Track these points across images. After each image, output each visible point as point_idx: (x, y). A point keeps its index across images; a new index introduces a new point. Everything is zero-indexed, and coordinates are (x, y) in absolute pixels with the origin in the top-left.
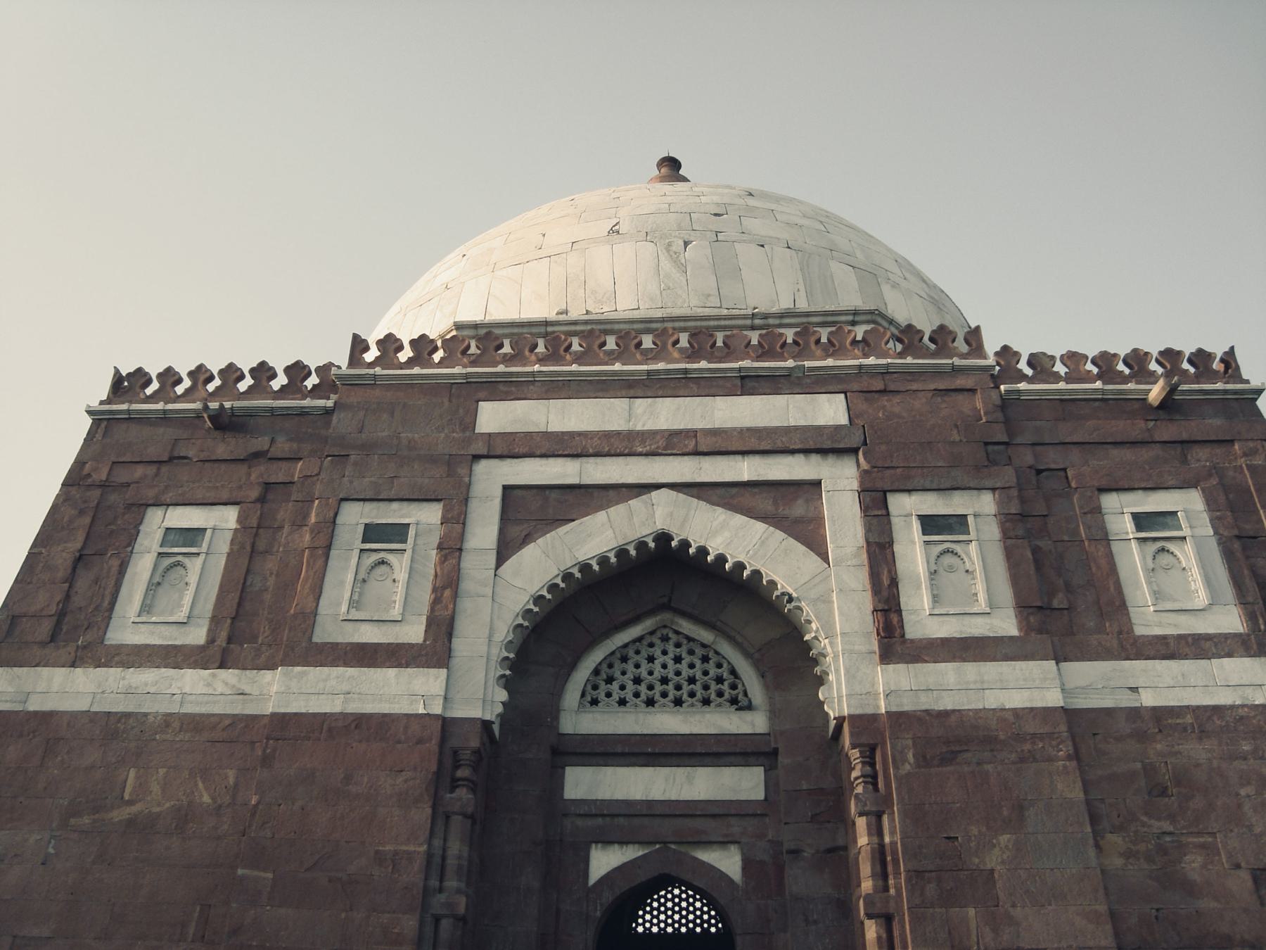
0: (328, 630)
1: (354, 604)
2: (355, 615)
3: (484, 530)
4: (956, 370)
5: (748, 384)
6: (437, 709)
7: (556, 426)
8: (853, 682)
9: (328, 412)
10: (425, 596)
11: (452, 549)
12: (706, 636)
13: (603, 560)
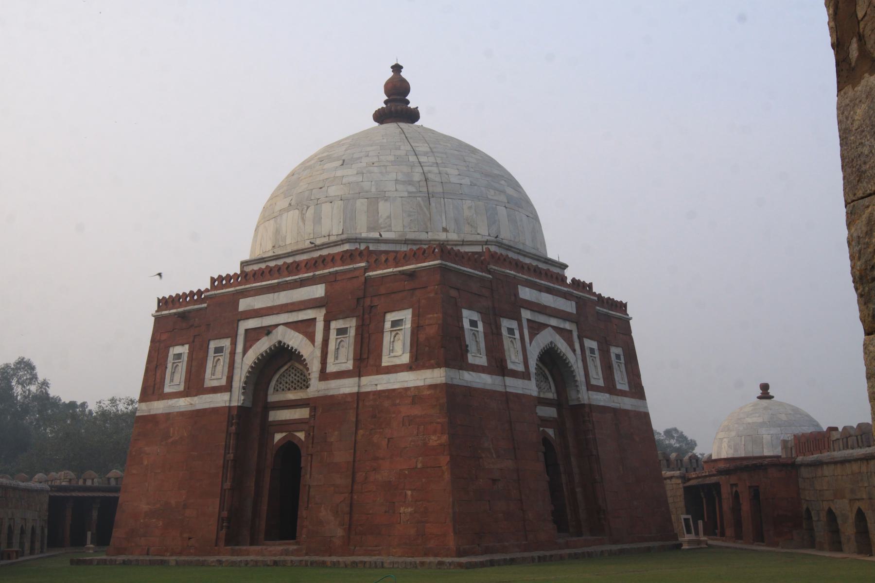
0: (209, 383)
1: (213, 374)
2: (213, 377)
3: (240, 348)
4: (355, 269)
5: (303, 283)
6: (227, 405)
7: (256, 307)
8: (316, 388)
9: (206, 308)
10: (226, 369)
11: (233, 353)
12: (301, 367)
13: (266, 352)
